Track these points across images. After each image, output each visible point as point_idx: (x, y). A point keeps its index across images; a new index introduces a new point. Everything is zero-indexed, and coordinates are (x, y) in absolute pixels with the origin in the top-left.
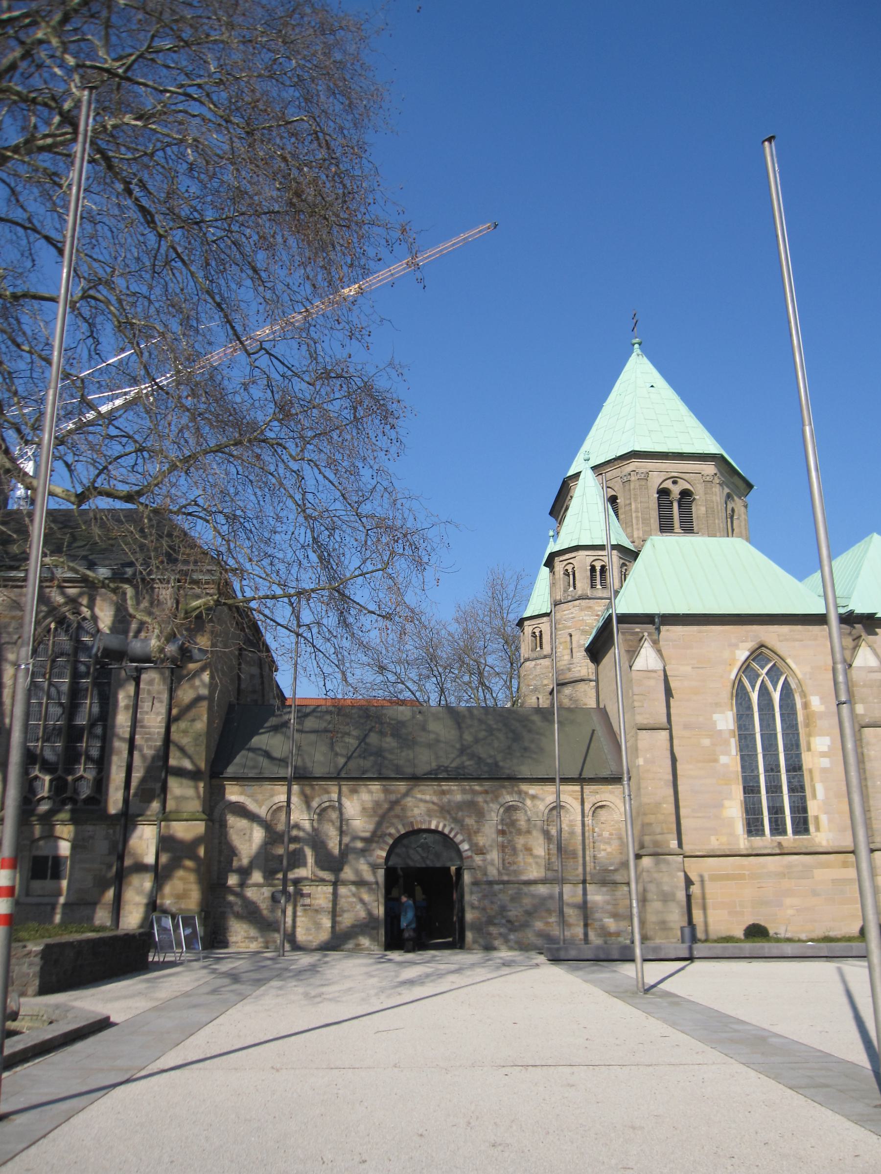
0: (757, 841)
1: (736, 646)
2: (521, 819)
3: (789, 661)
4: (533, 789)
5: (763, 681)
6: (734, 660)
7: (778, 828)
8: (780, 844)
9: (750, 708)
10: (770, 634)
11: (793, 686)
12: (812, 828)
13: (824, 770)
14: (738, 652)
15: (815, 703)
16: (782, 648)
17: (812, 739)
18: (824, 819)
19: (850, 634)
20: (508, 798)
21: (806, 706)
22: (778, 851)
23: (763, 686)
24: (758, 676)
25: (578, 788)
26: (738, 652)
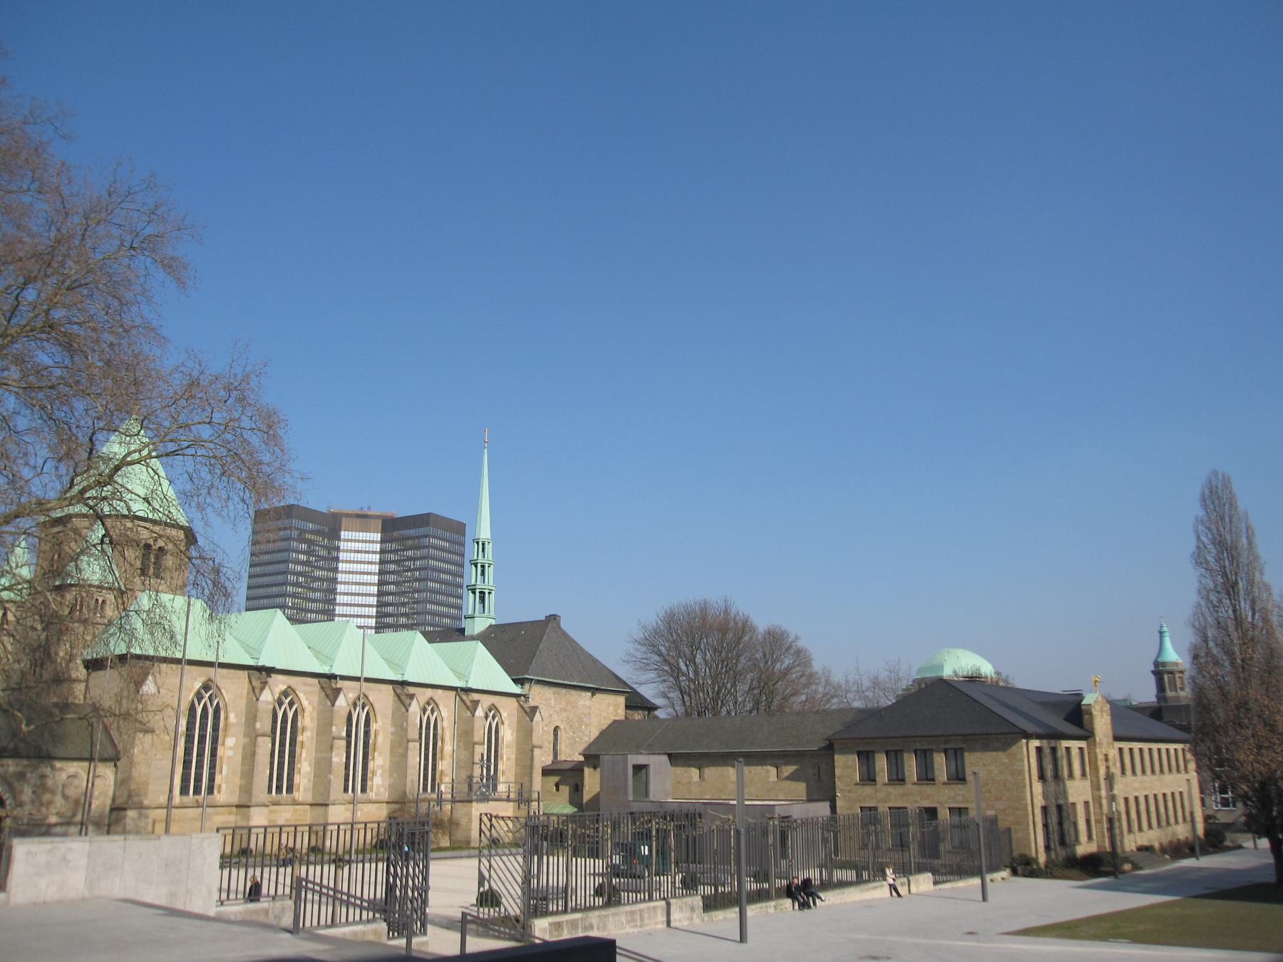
0: (185, 799)
1: (195, 679)
2: (50, 782)
3: (223, 691)
4: (58, 764)
5: (205, 703)
6: (193, 687)
7: (197, 791)
8: (197, 801)
9: (195, 717)
10: (211, 672)
11: (221, 705)
12: (215, 791)
13: (229, 758)
14: (196, 683)
15: (232, 717)
16: (220, 682)
17: (226, 740)
18: (224, 786)
19: (259, 678)
20: (48, 771)
21: (226, 718)
22: (196, 805)
23: (205, 705)
24: (202, 698)
25: (86, 764)
26: (196, 683)
